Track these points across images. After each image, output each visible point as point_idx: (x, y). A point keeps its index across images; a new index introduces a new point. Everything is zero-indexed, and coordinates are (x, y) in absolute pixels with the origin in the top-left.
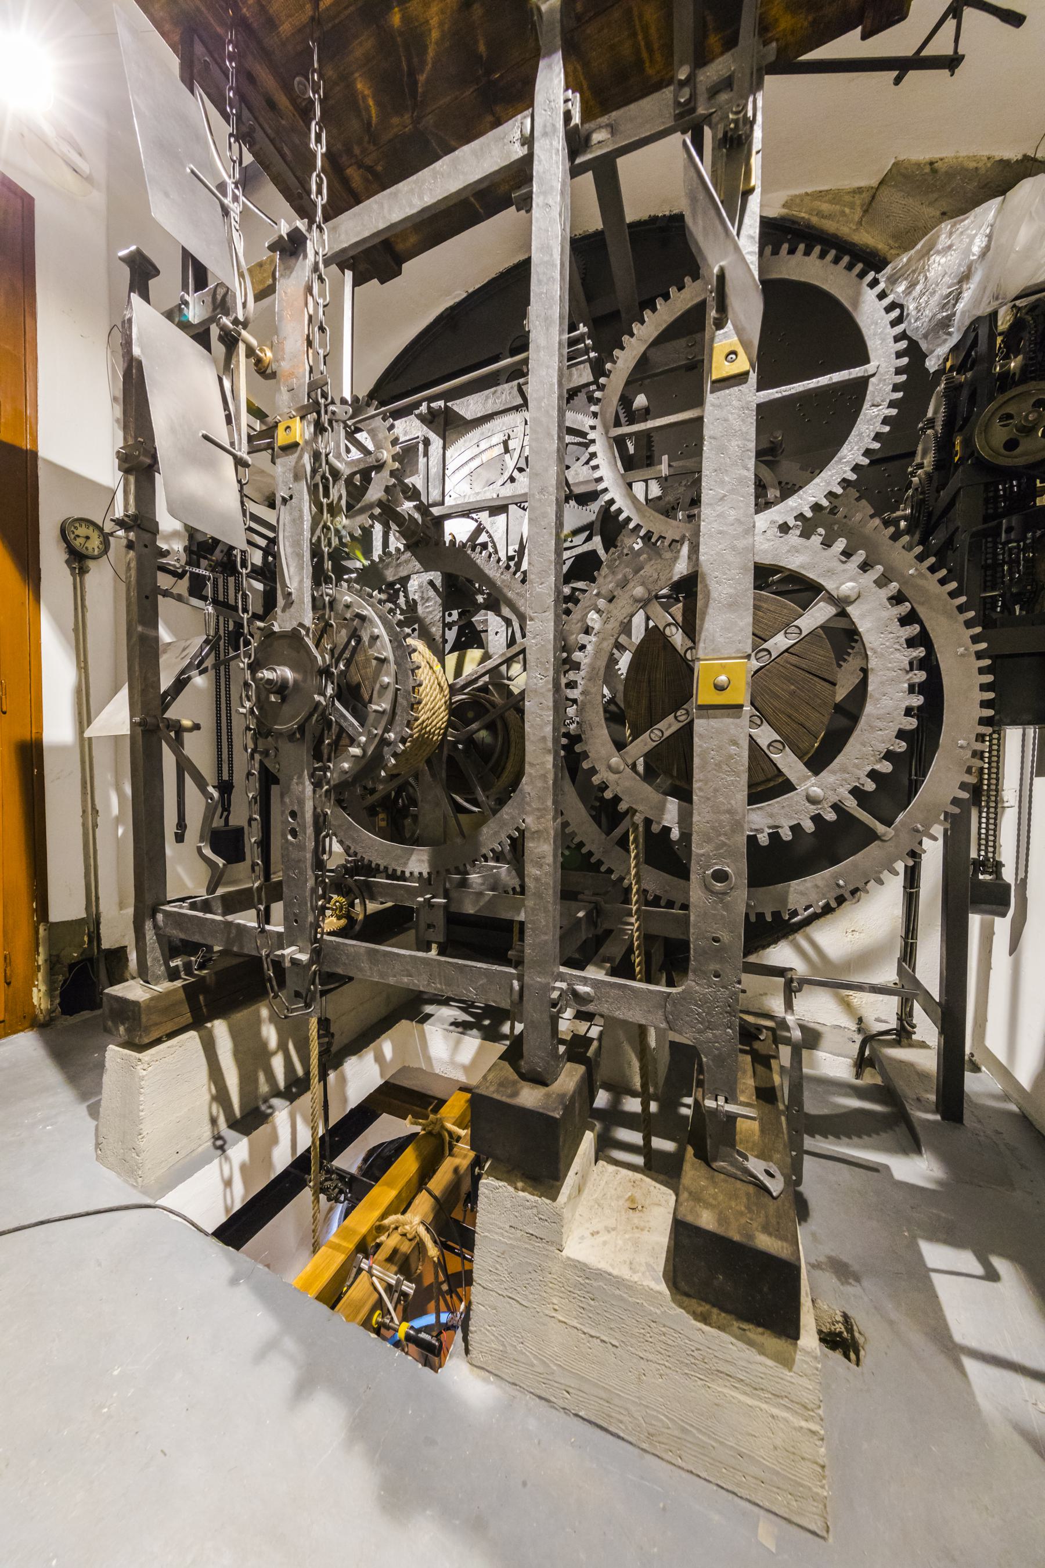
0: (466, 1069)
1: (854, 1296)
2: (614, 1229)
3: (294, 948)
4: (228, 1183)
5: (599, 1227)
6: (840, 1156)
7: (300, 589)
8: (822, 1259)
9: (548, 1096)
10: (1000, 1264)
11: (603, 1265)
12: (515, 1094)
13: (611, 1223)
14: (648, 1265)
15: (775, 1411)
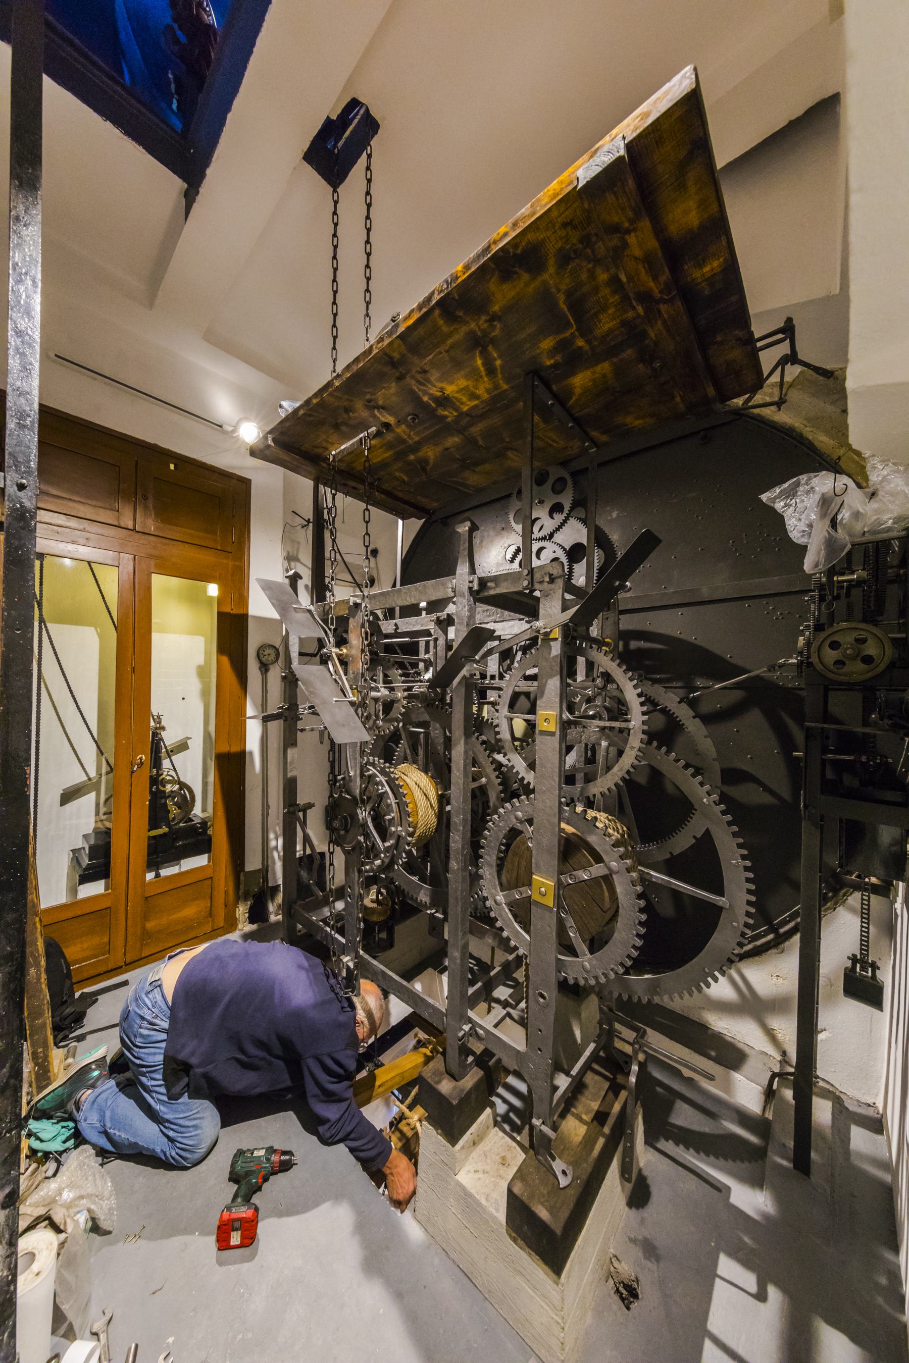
1: (649, 1269)
3: (348, 958)
7: (355, 775)
8: (640, 1237)
9: (455, 1088)
10: (773, 1292)
11: (473, 1191)
12: (439, 1082)
13: (488, 1168)
15: (543, 1304)
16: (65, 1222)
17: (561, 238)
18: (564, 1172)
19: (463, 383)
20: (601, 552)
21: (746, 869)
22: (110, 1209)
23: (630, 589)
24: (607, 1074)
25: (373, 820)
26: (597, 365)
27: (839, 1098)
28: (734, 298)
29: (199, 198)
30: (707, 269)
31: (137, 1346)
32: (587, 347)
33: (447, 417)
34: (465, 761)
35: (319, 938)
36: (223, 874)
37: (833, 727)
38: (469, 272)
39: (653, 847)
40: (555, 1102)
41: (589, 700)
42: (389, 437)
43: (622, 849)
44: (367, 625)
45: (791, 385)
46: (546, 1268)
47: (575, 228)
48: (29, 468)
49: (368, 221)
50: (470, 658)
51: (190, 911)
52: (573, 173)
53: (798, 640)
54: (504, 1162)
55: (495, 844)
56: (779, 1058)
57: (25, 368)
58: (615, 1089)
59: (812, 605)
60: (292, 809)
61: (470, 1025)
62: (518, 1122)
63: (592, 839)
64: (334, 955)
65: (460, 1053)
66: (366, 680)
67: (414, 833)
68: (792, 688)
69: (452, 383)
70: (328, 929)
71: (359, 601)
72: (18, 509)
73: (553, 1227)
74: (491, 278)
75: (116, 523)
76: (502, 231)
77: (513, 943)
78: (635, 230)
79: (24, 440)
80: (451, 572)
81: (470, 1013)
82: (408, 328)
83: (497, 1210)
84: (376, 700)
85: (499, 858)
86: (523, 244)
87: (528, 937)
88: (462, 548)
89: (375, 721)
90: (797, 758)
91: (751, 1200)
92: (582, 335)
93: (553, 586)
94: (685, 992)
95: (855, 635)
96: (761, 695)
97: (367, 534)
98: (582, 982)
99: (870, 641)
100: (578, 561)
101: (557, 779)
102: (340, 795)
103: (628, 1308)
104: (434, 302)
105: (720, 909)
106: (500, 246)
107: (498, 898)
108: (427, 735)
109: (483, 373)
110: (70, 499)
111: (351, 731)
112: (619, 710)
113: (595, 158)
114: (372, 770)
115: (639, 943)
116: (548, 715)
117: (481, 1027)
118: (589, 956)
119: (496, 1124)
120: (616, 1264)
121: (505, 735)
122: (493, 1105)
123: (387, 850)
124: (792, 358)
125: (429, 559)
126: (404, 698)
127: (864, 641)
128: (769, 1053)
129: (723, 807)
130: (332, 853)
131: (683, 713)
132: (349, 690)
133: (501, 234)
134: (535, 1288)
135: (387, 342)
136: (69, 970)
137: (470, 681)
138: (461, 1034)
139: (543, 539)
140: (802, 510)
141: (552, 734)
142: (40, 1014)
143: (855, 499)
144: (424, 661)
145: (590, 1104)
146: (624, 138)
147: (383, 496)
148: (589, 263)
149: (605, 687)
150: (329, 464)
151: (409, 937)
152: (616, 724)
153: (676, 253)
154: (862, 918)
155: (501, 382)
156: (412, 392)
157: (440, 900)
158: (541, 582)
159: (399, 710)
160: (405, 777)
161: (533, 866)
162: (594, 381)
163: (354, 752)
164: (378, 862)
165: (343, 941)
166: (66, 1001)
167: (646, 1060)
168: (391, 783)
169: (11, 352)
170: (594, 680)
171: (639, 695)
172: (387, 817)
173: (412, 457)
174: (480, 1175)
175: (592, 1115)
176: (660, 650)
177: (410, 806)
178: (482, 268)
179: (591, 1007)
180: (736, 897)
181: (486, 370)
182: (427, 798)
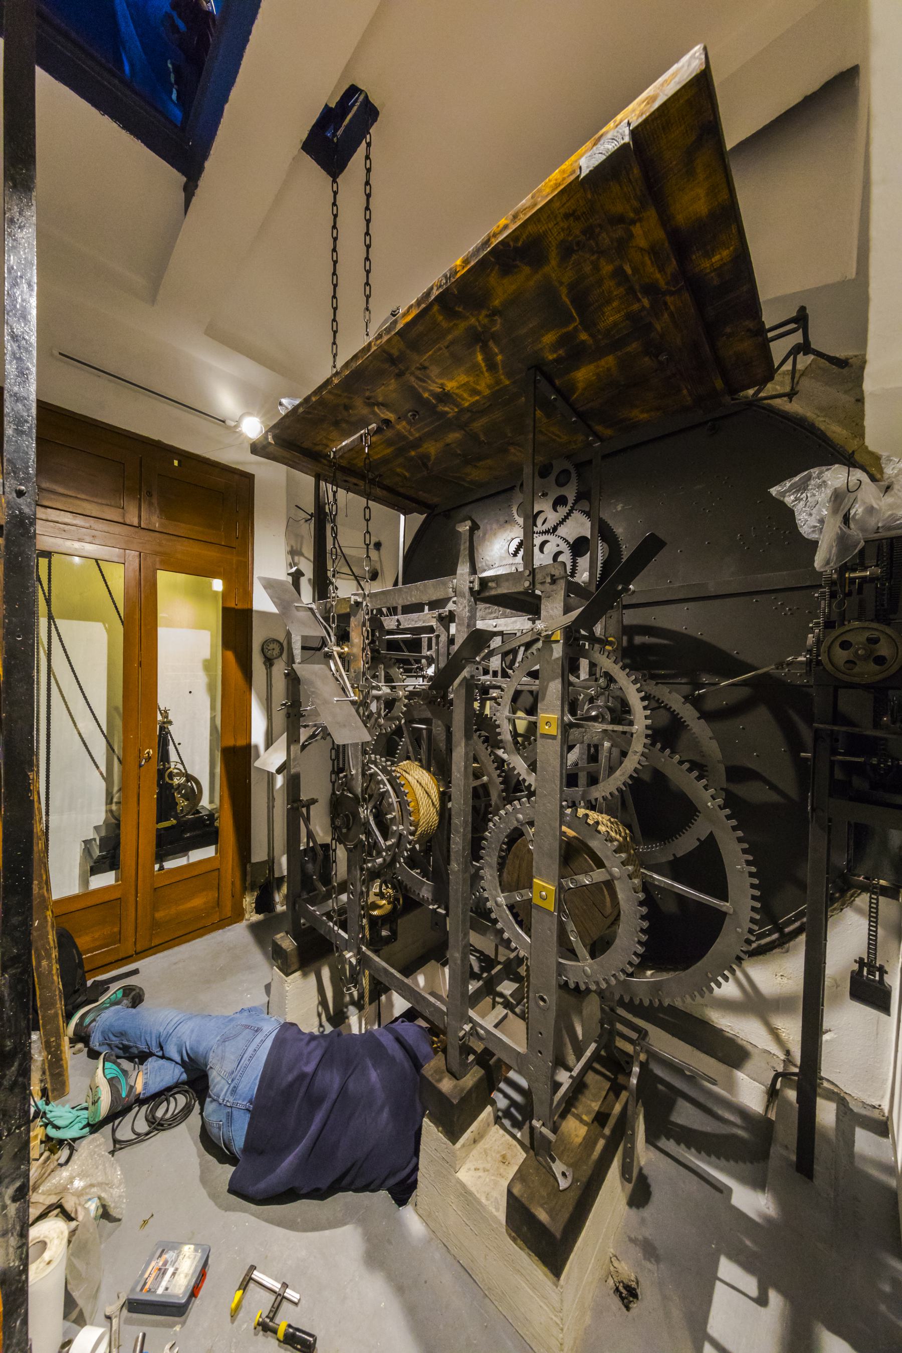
1: (650, 1270)
2: (488, 1171)
3: (351, 954)
5: (481, 1166)
6: (699, 1171)
7: (357, 773)
8: (640, 1237)
9: (455, 1087)
10: (774, 1297)
12: (440, 1080)
13: (488, 1166)
14: (496, 1198)
15: (542, 1304)
16: (76, 1211)
17: (563, 230)
18: (564, 1174)
19: (463, 378)
20: (605, 545)
21: (751, 875)
22: (120, 1196)
23: (634, 592)
24: (608, 1073)
26: (600, 359)
27: (843, 1099)
28: (745, 288)
29: (198, 192)
30: (717, 257)
31: (144, 1335)
32: (590, 341)
33: (447, 413)
34: (465, 763)
35: (322, 932)
37: (844, 729)
38: (469, 267)
39: (656, 848)
40: (555, 1103)
41: (591, 700)
42: (389, 433)
43: (623, 855)
44: (368, 624)
45: (803, 374)
46: (546, 1269)
47: (577, 219)
48: (28, 473)
49: (368, 212)
50: (470, 660)
51: (198, 902)
52: (576, 161)
53: (806, 638)
54: (504, 1160)
55: (495, 846)
56: (783, 1057)
57: (22, 373)
58: (616, 1089)
59: (823, 602)
60: (295, 805)
61: (471, 1025)
62: (520, 1118)
63: (594, 844)
64: (337, 951)
65: (461, 1054)
66: (367, 679)
67: (416, 830)
68: (800, 686)
69: (452, 379)
70: (331, 924)
71: (359, 600)
72: (17, 516)
73: (552, 1229)
74: (491, 271)
75: (121, 521)
76: (502, 224)
77: (513, 945)
78: (640, 220)
79: (24, 445)
80: (452, 571)
81: (471, 1013)
82: (407, 325)
83: (497, 1210)
84: (378, 698)
85: (500, 857)
86: (524, 237)
87: (528, 940)
88: (462, 548)
89: (376, 720)
90: (806, 759)
91: (752, 1202)
92: (586, 329)
93: (554, 587)
94: (687, 996)
95: (867, 634)
96: (768, 692)
97: (368, 532)
98: (583, 987)
99: (882, 641)
100: (581, 555)
101: (558, 782)
102: (342, 794)
103: (628, 1308)
104: (433, 298)
105: (725, 914)
106: (500, 239)
107: (499, 899)
108: (429, 731)
109: (484, 369)
110: (76, 497)
111: (352, 733)
112: (620, 712)
113: (599, 146)
114: (374, 769)
115: (640, 950)
116: (550, 719)
118: (590, 961)
119: (497, 1120)
120: (616, 1264)
121: (507, 737)
122: (493, 1103)
123: (389, 848)
124: (804, 348)
125: (431, 556)
126: (406, 697)
127: (876, 641)
128: (772, 1052)
129: (728, 811)
131: (688, 713)
132: (350, 689)
133: (501, 226)
134: (534, 1288)
135: (385, 338)
136: (81, 960)
137: (472, 682)
138: (461, 1034)
139: (547, 532)
140: (813, 504)
141: (553, 737)
142: (53, 1005)
143: (869, 494)
144: (427, 658)
145: (591, 1104)
146: (629, 124)
147: (385, 492)
148: (593, 254)
149: (608, 686)
150: (330, 461)
151: (411, 931)
152: (619, 728)
153: (682, 243)
154: (870, 921)
155: (502, 377)
156: (412, 389)
157: (441, 896)
158: (543, 583)
159: (401, 708)
160: (407, 775)
161: (534, 869)
162: (598, 375)
166: (78, 990)
167: (647, 1060)
168: (392, 781)
169: (8, 357)
170: (596, 680)
171: (643, 699)
172: (389, 816)
173: (413, 453)
174: (480, 1173)
175: (593, 1115)
176: (665, 646)
177: (412, 804)
178: (482, 263)
179: (592, 1006)
180: (740, 902)
181: (486, 366)
182: (429, 795)
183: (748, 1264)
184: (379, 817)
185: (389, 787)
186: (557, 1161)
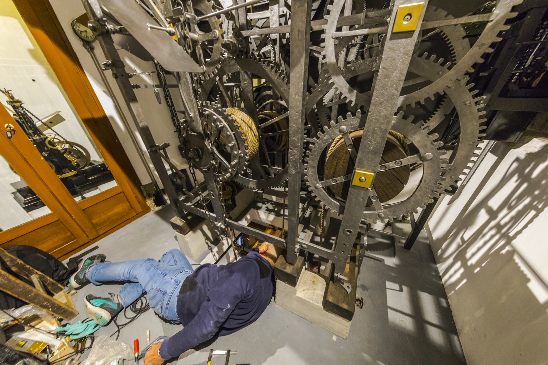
0: (271, 222)
4: (214, 255)
7: (195, 115)
9: (293, 269)
11: (305, 299)
12: (285, 268)
13: (308, 287)
18: (348, 287)
25: (217, 148)
36: (129, 189)
60: (153, 149)
83: (318, 303)
91: (391, 261)
114: (208, 111)
117: (305, 244)
123: (233, 167)
130: (194, 173)
163: (188, 95)
164: (228, 175)
165: (215, 215)
168: (226, 118)
172: (230, 145)
182: (251, 129)
183: (394, 280)
184: (221, 148)
185: (225, 123)
186: (345, 283)
